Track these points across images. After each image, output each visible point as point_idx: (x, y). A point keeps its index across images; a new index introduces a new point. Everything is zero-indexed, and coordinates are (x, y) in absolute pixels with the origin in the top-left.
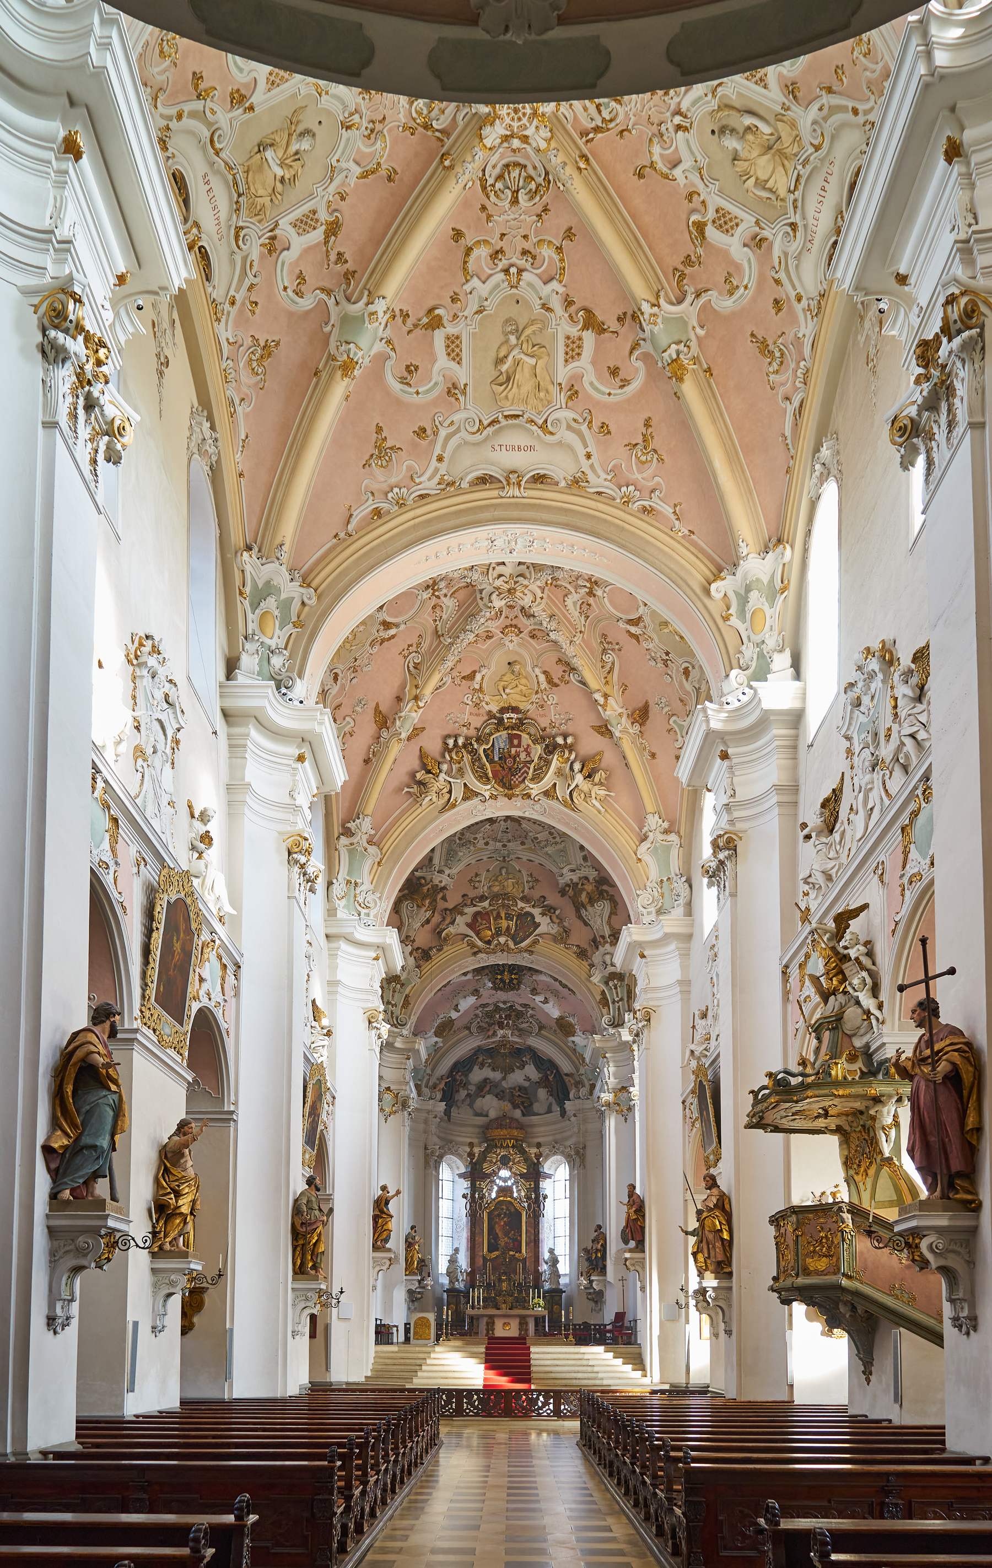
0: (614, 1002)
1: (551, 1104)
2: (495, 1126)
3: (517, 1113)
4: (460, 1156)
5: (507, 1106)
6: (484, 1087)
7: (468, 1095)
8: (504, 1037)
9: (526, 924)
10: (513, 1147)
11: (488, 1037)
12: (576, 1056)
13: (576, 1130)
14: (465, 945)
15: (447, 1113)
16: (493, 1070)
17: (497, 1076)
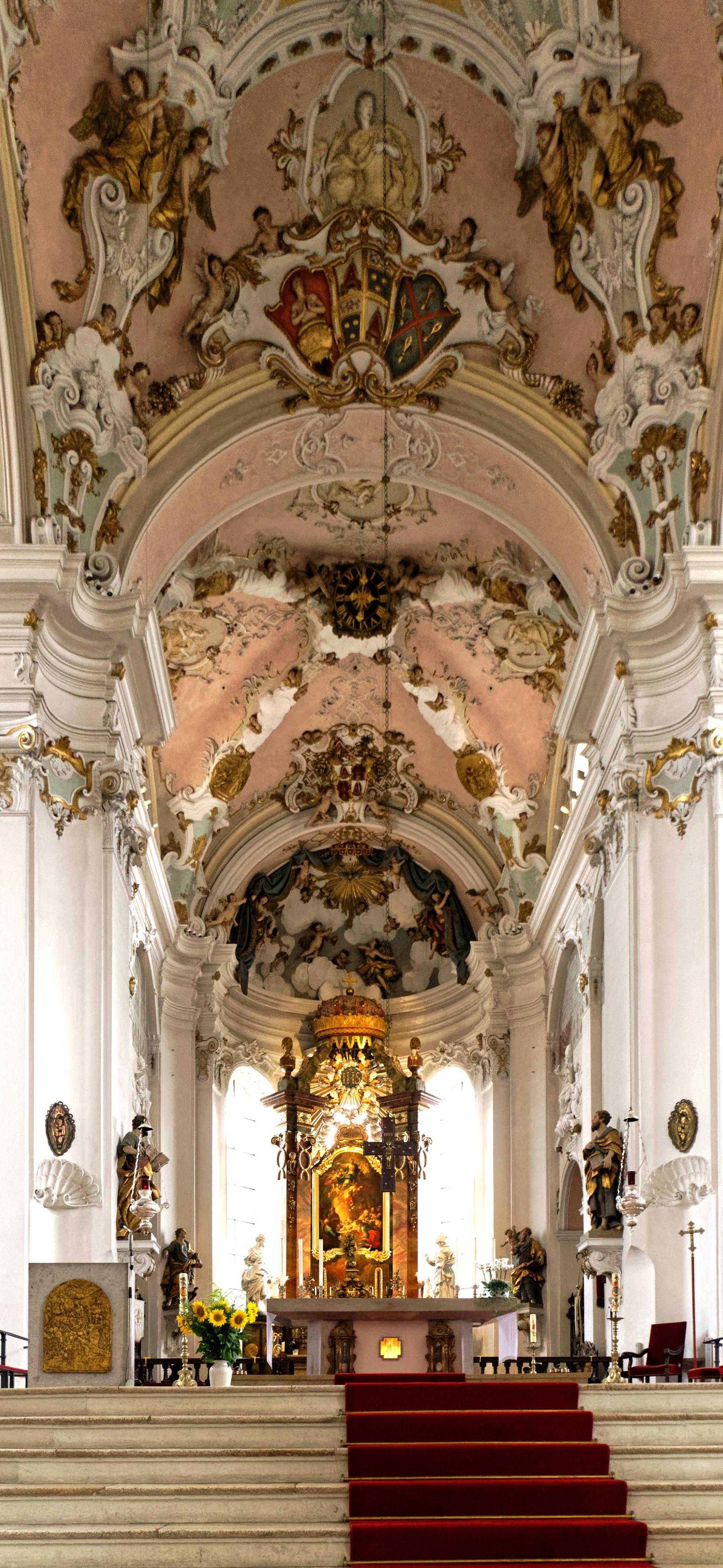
0: (650, 523)
1: (436, 972)
2: (332, 1009)
3: (374, 992)
4: (264, 1069)
5: (355, 981)
6: (314, 941)
7: (282, 956)
8: (350, 819)
9: (422, 306)
10: (367, 1051)
11: (320, 817)
12: (490, 846)
13: (488, 1005)
14: (265, 373)
15: (241, 975)
16: (328, 904)
17: (334, 918)
